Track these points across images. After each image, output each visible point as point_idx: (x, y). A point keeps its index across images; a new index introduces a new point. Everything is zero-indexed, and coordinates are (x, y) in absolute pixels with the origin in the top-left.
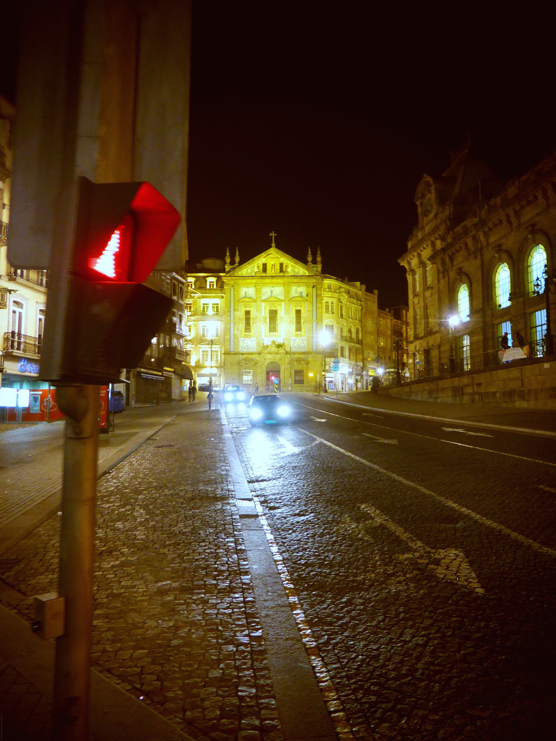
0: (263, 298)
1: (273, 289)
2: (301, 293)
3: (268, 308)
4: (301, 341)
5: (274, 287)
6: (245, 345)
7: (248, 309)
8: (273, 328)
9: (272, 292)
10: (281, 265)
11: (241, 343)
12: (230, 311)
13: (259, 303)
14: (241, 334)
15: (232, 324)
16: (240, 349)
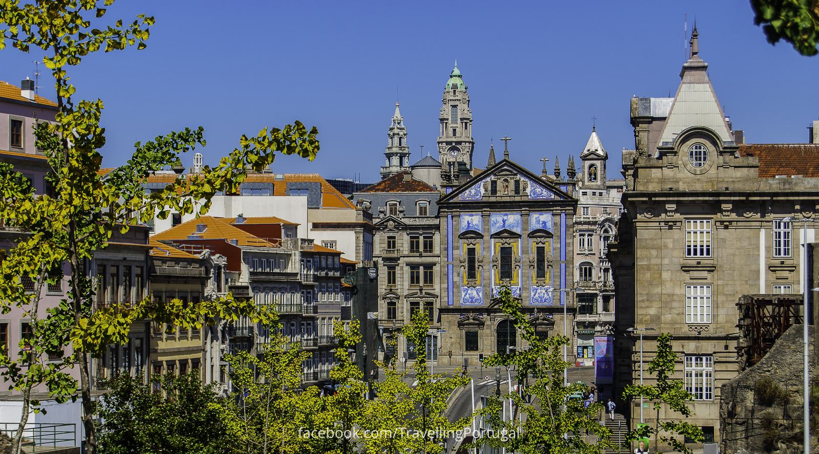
0: (493, 231)
1: (505, 218)
2: (544, 223)
3: (499, 246)
4: (544, 291)
5: (507, 215)
7: (471, 246)
8: (506, 272)
9: (504, 221)
10: (517, 183)
11: (463, 294)
12: (447, 249)
13: (487, 238)
14: (463, 282)
15: (450, 267)
16: (461, 301)
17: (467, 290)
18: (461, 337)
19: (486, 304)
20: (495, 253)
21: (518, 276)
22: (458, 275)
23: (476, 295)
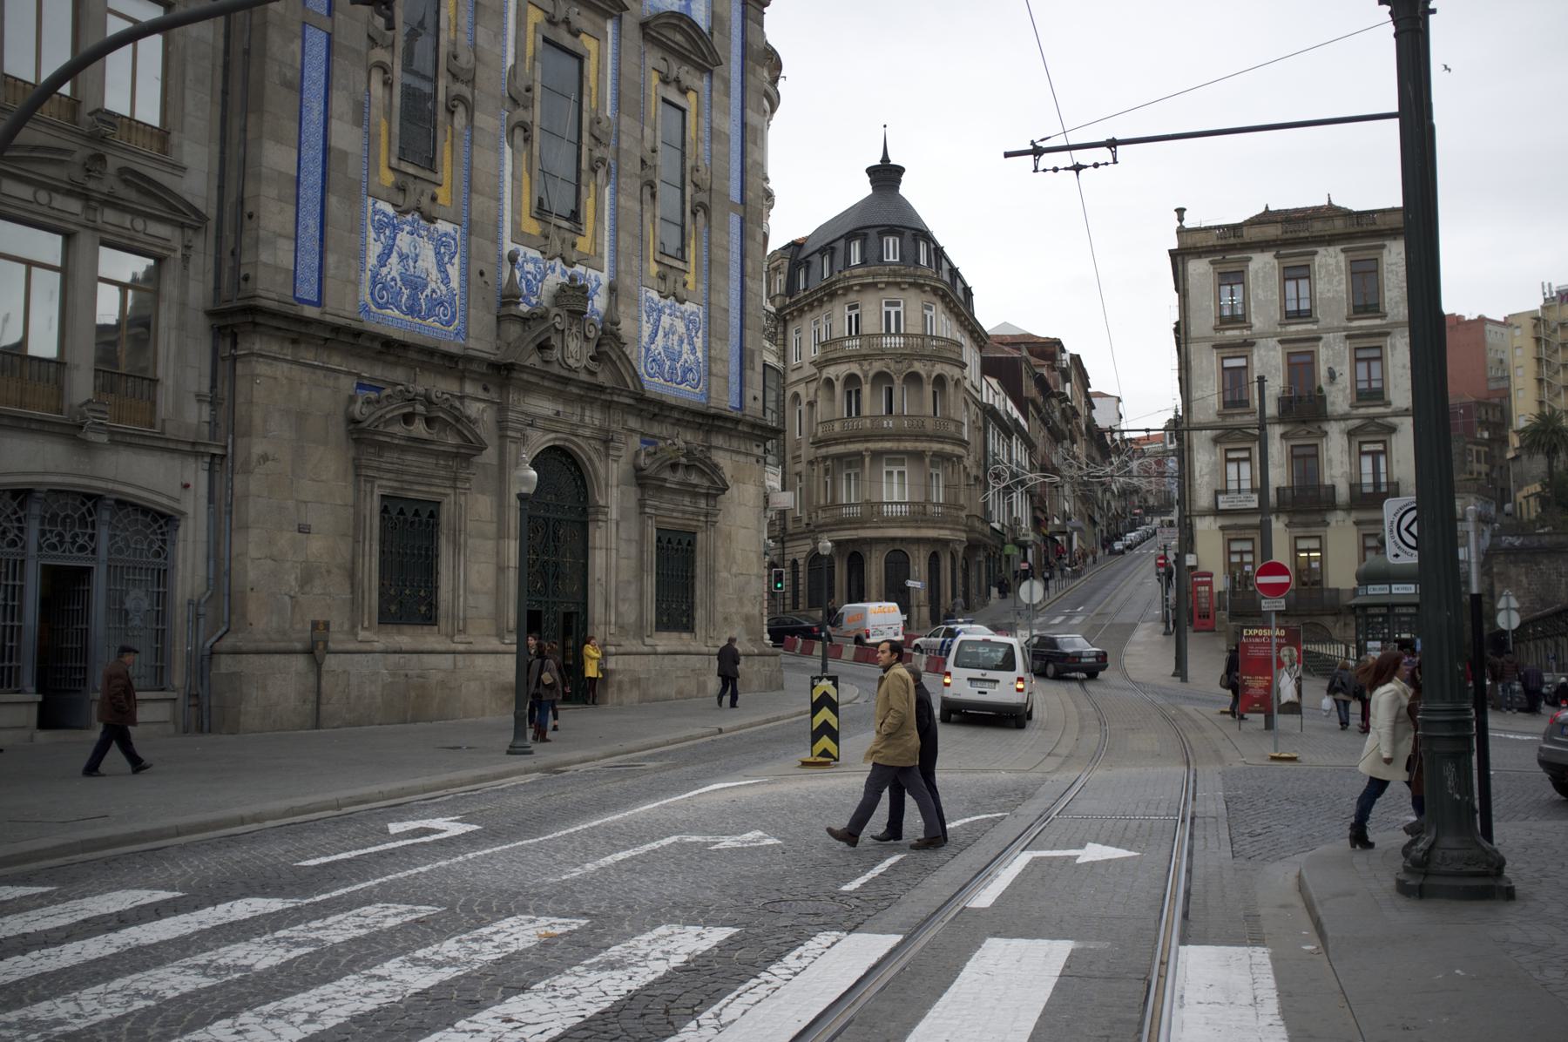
6: (394, 267)
11: (374, 250)
17: (396, 229)
18: (356, 533)
19: (481, 340)
20: (519, 55)
21: (598, 218)
22: (360, 114)
23: (435, 274)
